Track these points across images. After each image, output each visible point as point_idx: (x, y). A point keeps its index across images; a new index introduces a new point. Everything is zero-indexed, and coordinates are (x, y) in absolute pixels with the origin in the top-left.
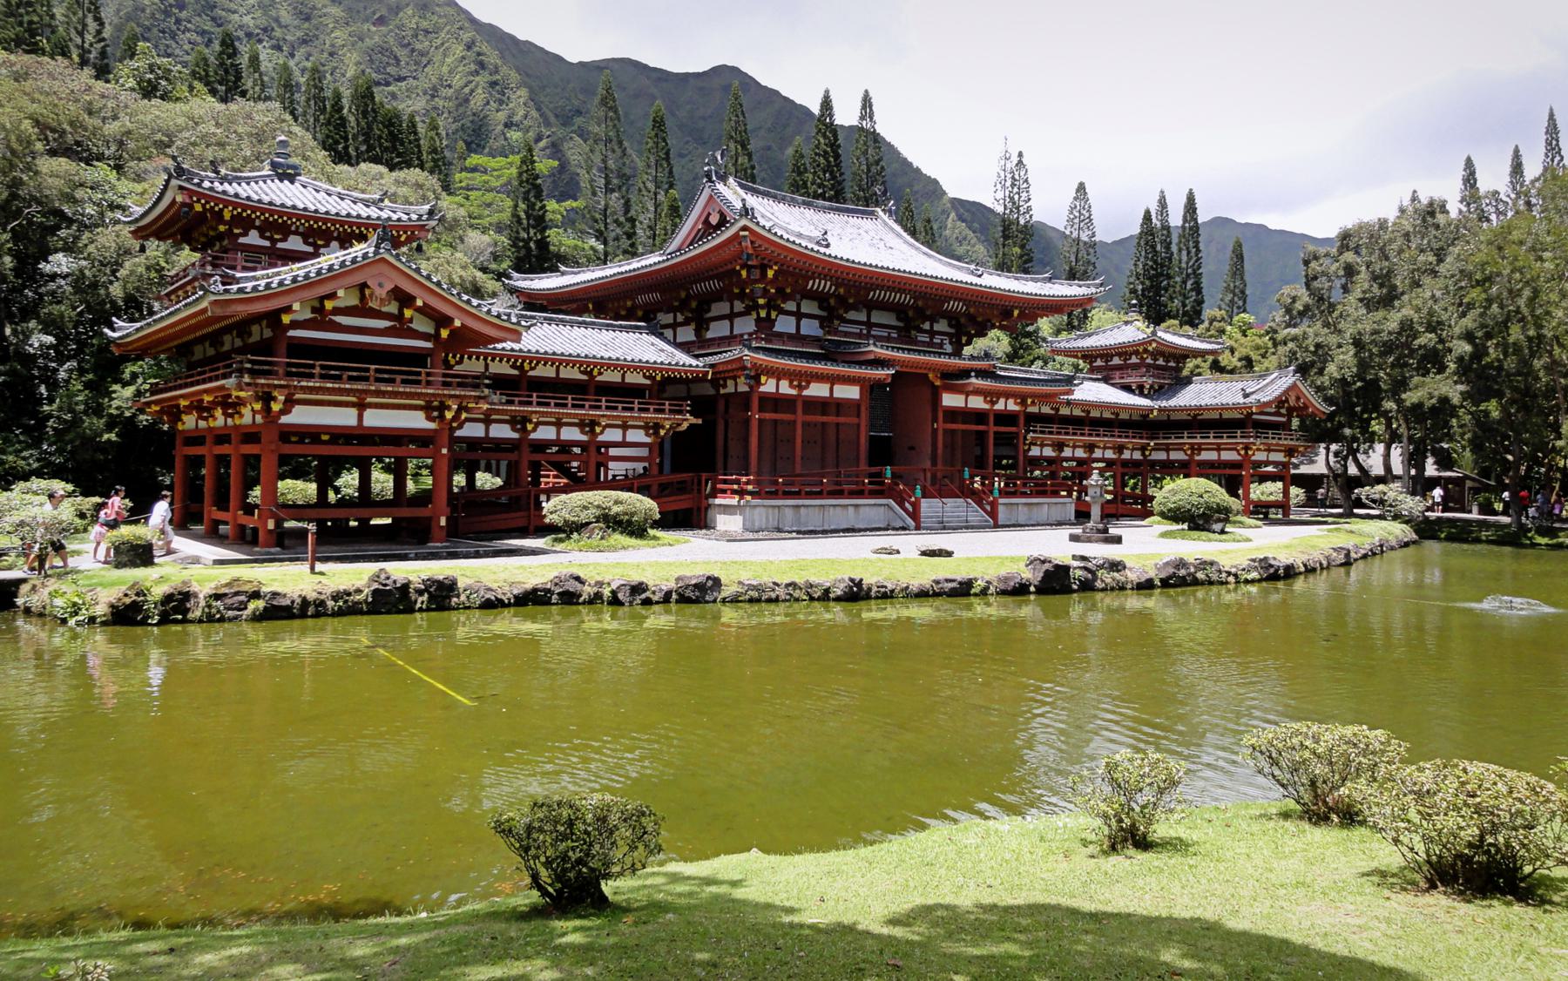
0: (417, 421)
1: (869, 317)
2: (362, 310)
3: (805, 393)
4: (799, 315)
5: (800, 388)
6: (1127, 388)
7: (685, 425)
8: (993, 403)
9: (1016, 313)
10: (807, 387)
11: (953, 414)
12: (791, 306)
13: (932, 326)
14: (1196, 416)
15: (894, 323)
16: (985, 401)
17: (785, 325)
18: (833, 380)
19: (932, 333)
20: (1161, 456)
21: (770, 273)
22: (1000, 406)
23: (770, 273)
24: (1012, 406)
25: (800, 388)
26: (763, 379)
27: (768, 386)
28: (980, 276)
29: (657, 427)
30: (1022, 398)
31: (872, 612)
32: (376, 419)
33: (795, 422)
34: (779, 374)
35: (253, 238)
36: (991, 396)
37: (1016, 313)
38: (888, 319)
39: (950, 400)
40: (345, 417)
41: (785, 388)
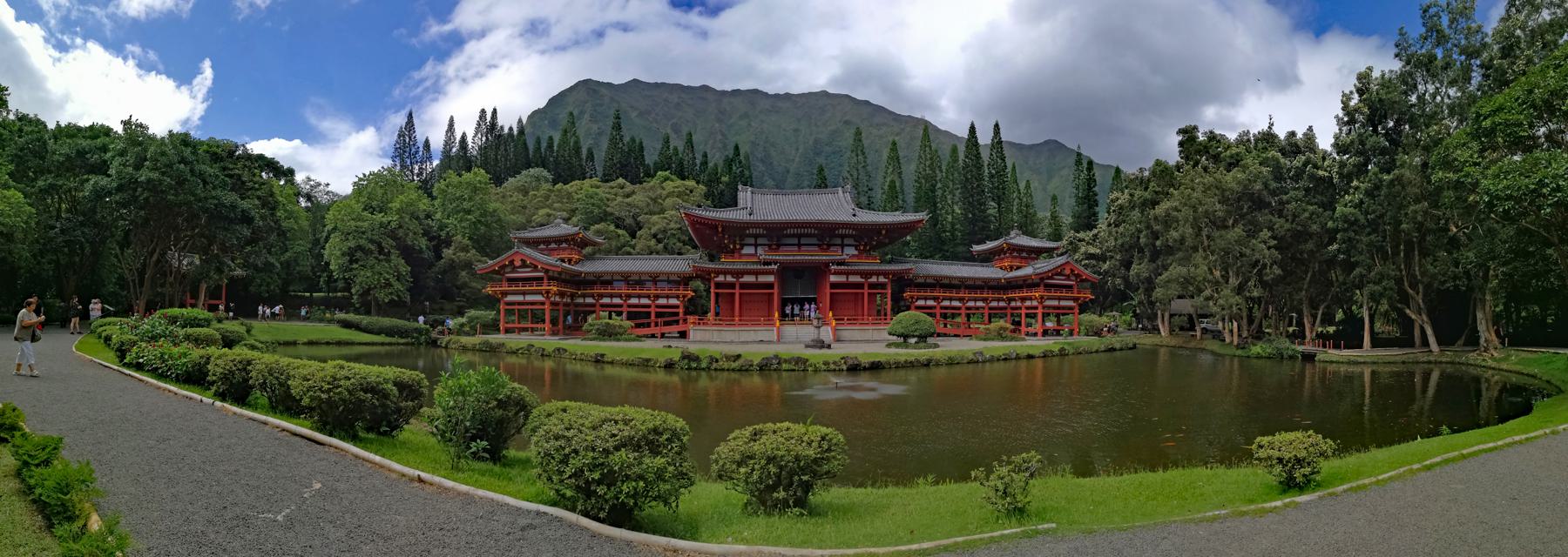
0: (539, 298)
1: (799, 241)
2: (524, 265)
3: (741, 280)
4: (756, 246)
5: (738, 278)
6: (1001, 268)
7: (689, 296)
8: (866, 278)
9: (884, 232)
10: (742, 277)
11: (834, 285)
12: (752, 241)
13: (843, 241)
14: (1025, 281)
15: (817, 242)
16: (862, 278)
17: (748, 250)
18: (756, 273)
19: (843, 246)
20: (1013, 304)
21: (720, 230)
22: (874, 279)
23: (720, 230)
24: (882, 279)
25: (738, 278)
26: (713, 275)
27: (721, 278)
28: (854, 215)
29: (684, 296)
30: (885, 274)
31: (609, 370)
32: (529, 298)
33: (734, 293)
34: (725, 272)
35: (542, 246)
36: (866, 274)
37: (884, 232)
38: (814, 241)
39: (833, 278)
40: (520, 298)
41: (730, 279)
